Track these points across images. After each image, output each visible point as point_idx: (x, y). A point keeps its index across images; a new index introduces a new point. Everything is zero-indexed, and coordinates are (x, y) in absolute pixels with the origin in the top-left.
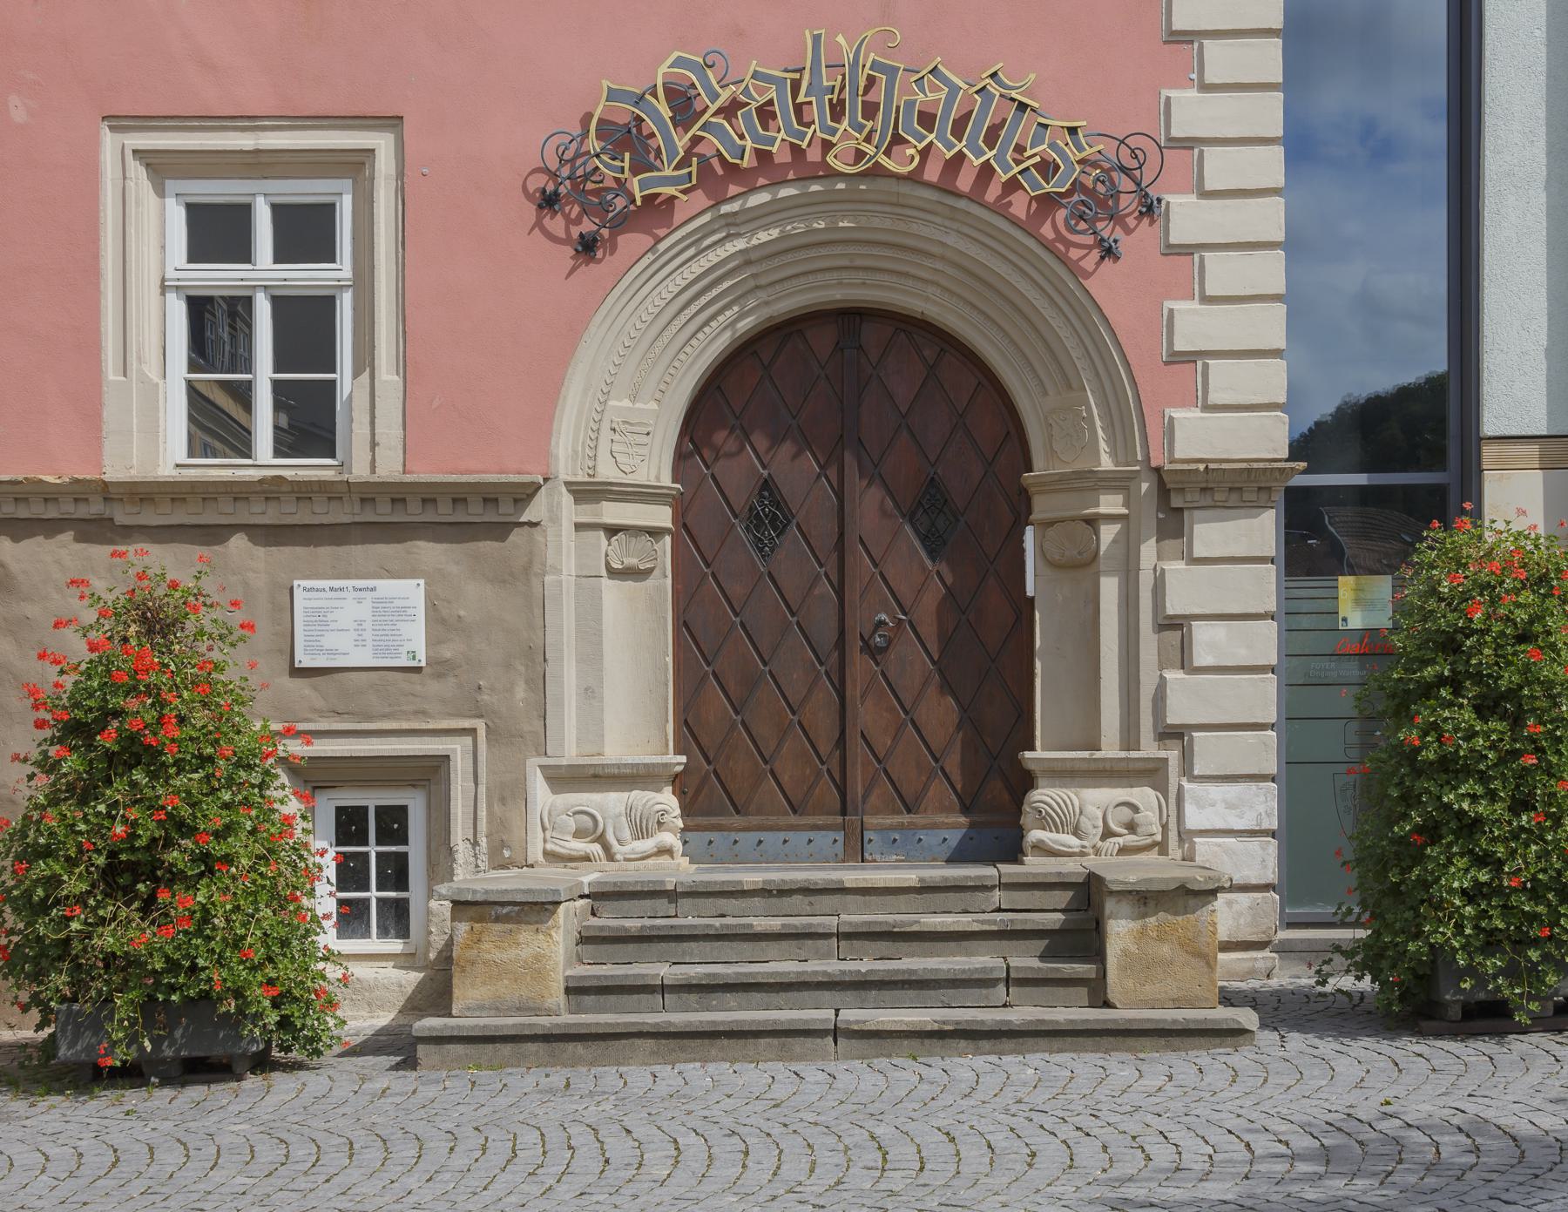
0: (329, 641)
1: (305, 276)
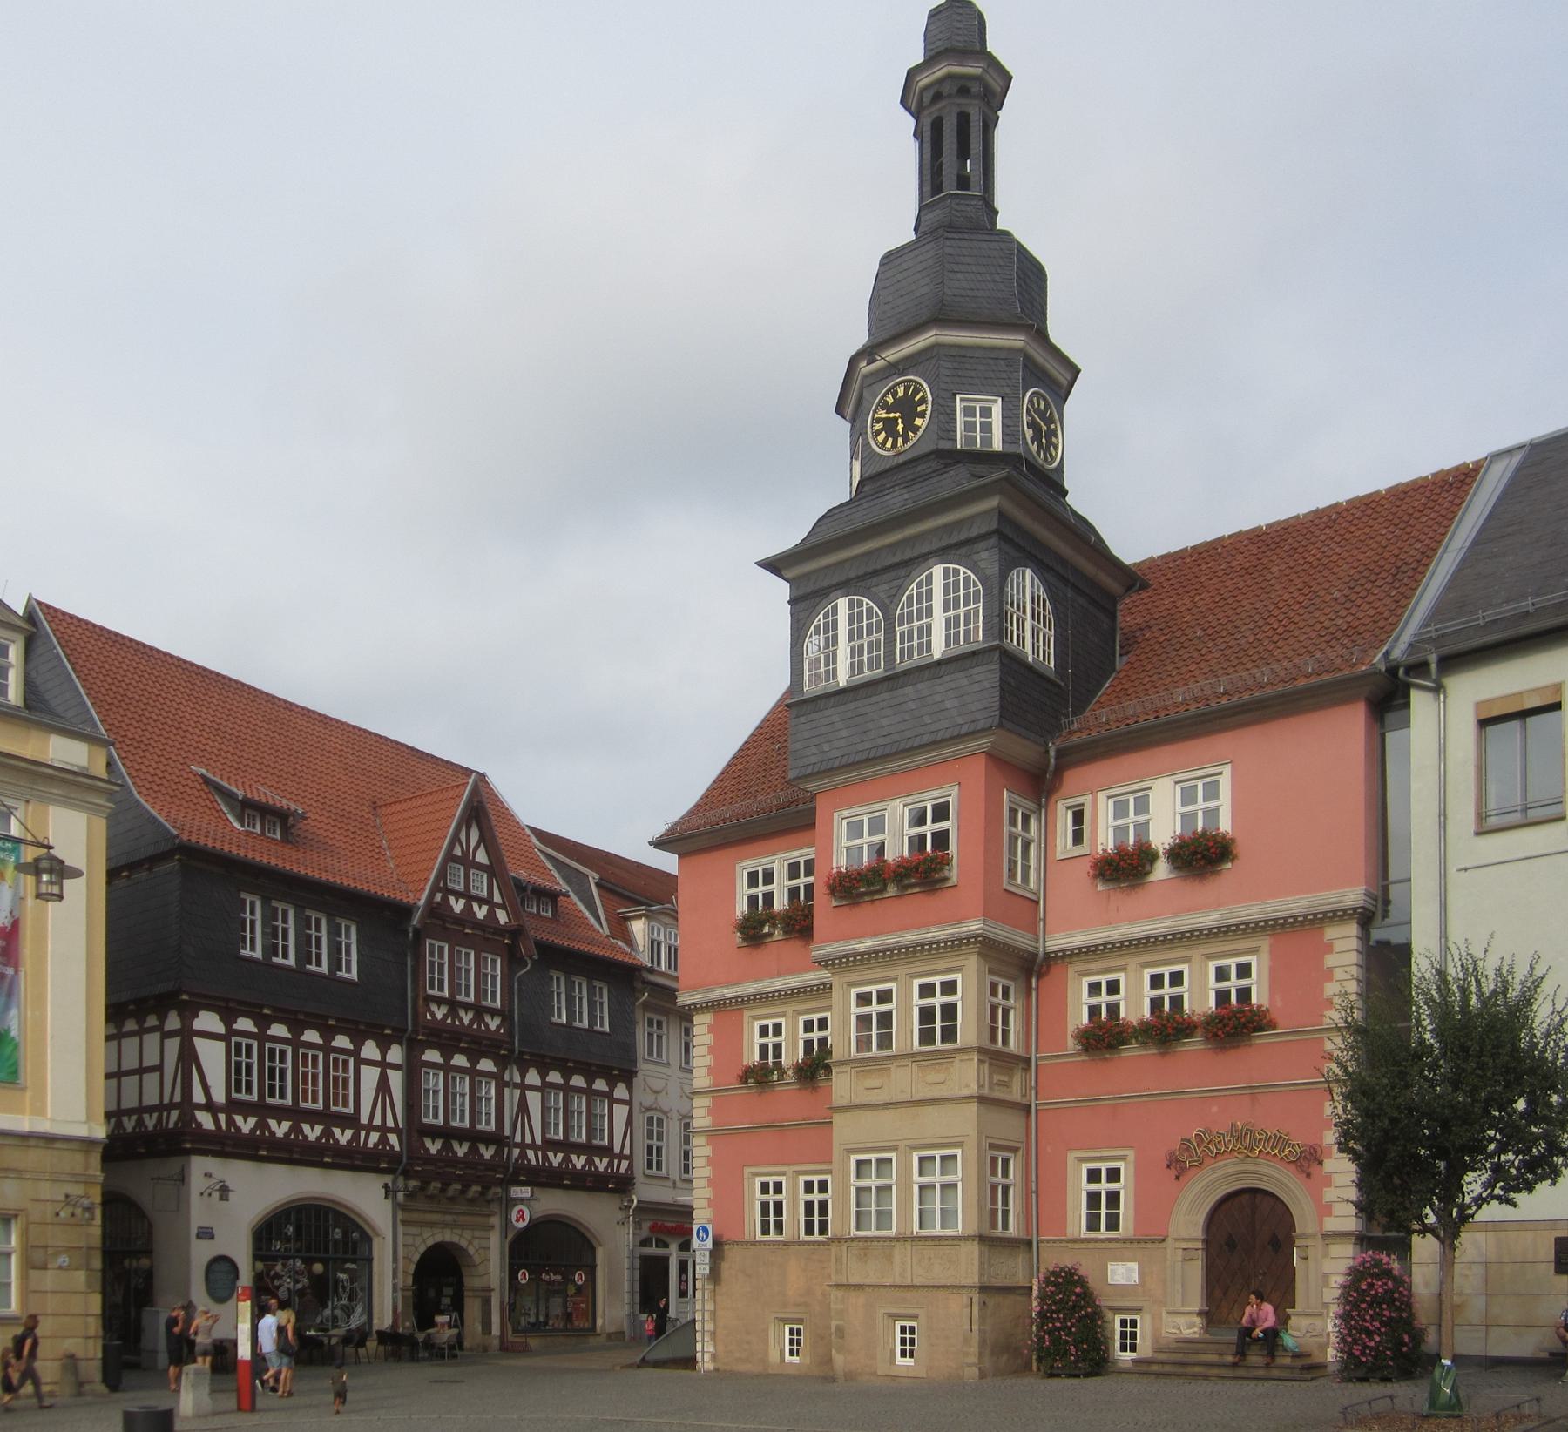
0: (1116, 1277)
1: (1113, 1186)
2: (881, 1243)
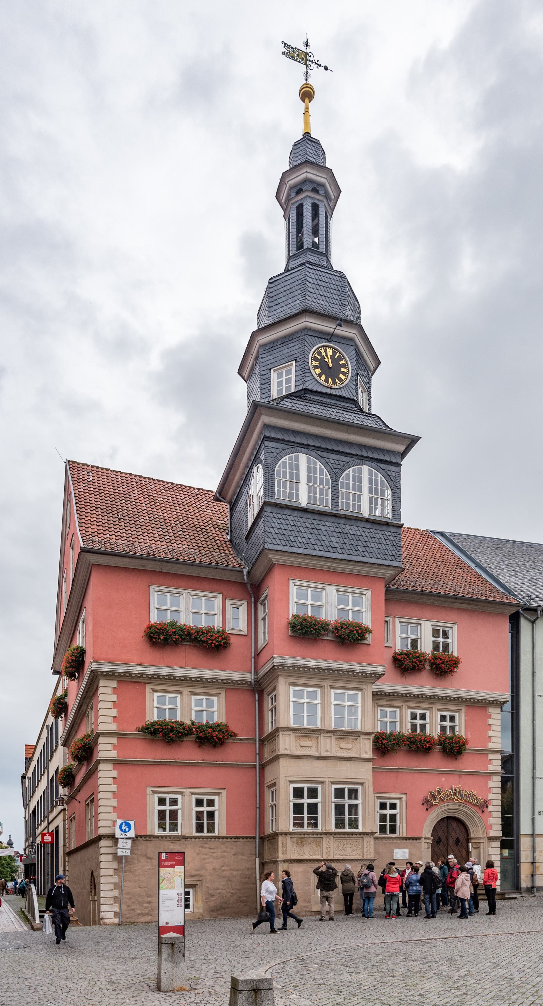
2: (315, 836)
